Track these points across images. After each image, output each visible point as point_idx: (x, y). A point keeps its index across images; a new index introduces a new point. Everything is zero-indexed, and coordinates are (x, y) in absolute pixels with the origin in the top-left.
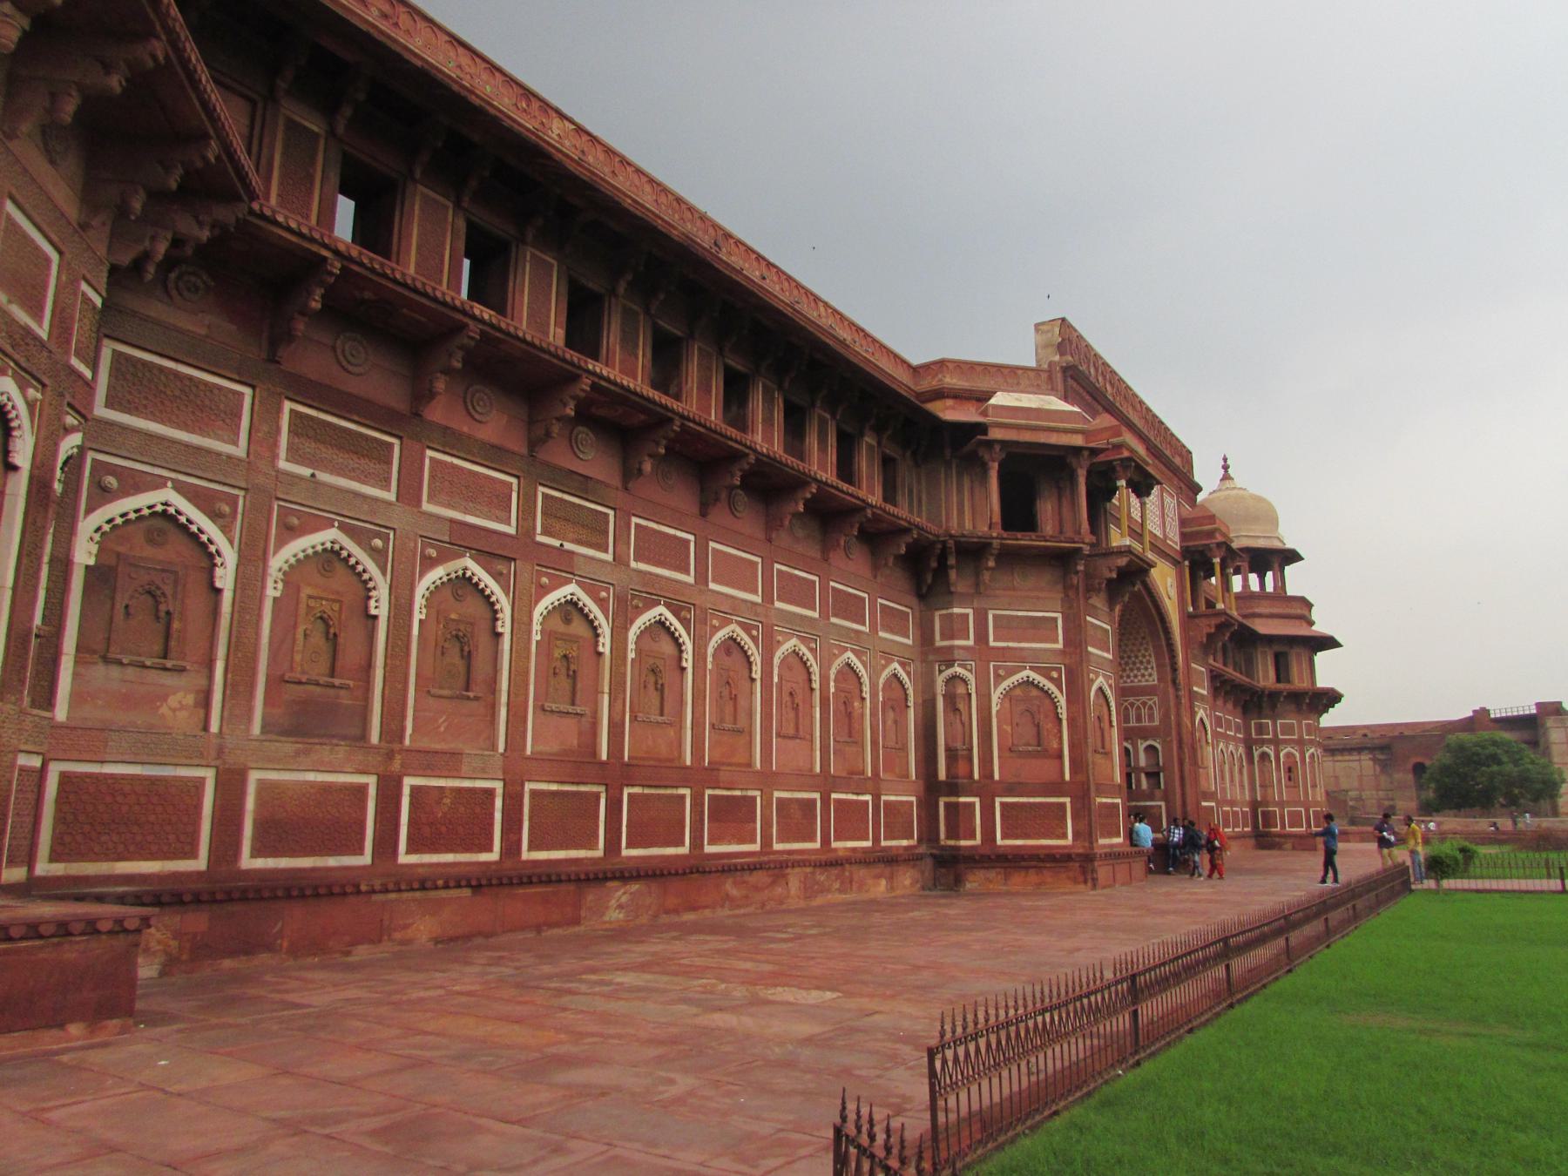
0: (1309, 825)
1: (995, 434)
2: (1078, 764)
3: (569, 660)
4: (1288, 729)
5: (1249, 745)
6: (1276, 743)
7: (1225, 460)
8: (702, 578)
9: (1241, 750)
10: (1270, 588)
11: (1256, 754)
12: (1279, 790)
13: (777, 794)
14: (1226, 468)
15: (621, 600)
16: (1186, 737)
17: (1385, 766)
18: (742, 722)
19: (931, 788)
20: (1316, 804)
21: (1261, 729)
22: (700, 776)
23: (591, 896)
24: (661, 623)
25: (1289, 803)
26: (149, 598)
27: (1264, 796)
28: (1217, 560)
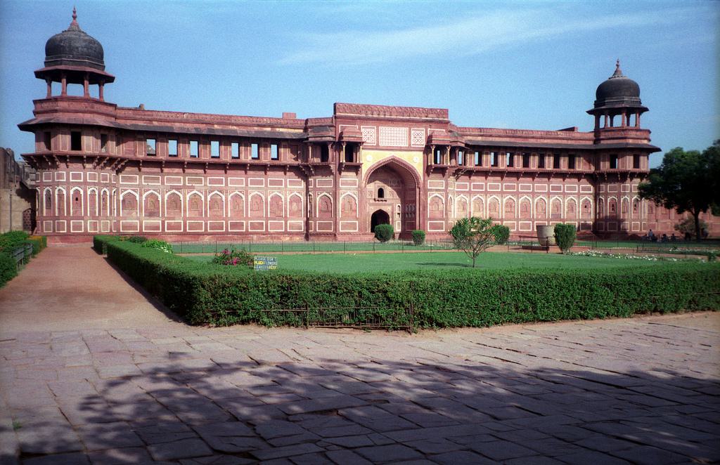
1: (310, 139)
3: (195, 202)
5: (596, 196)
8: (226, 184)
13: (244, 222)
14: (617, 65)
15: (206, 192)
18: (241, 208)
19: (308, 219)
22: (226, 219)
26: (129, 202)
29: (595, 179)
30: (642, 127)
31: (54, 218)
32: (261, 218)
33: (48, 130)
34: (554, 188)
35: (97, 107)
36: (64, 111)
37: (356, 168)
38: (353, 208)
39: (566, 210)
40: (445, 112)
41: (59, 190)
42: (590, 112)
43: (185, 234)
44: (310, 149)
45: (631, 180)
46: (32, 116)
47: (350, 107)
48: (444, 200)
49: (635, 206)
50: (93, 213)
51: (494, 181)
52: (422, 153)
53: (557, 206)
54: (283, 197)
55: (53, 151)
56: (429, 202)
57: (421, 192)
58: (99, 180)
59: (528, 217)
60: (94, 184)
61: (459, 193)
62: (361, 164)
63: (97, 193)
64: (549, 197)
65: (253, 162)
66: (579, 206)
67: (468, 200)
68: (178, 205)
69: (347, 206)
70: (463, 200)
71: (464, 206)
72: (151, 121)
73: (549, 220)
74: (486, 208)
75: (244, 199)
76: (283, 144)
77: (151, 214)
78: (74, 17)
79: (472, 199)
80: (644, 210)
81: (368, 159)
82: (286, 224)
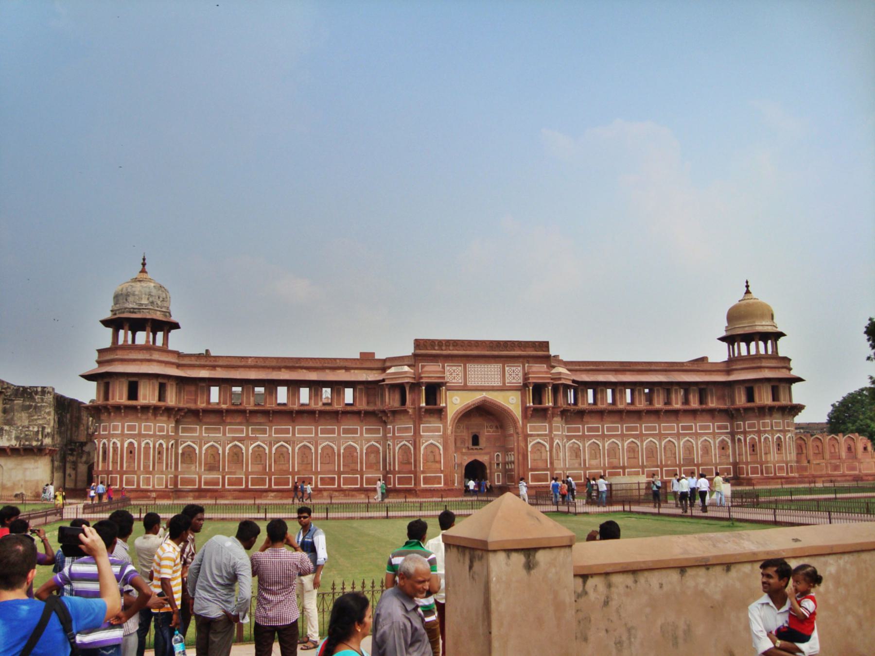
0: (762, 473)
1: (387, 382)
2: (415, 466)
5: (732, 434)
6: (745, 433)
7: (747, 282)
8: (294, 434)
10: (770, 352)
14: (747, 286)
15: (270, 443)
16: (521, 451)
18: (309, 461)
20: (767, 462)
21: (738, 427)
22: (293, 474)
23: (265, 494)
24: (282, 445)
25: (751, 463)
26: (189, 456)
29: (731, 414)
30: (781, 354)
31: (108, 473)
32: (334, 472)
33: (106, 380)
34: (684, 428)
35: (156, 356)
36: (123, 361)
37: (440, 413)
38: (437, 459)
40: (545, 345)
41: (114, 443)
42: (722, 339)
43: (247, 490)
44: (387, 390)
45: (771, 415)
46: (96, 365)
47: (432, 343)
48: (548, 446)
49: (779, 445)
50: (146, 467)
51: (613, 423)
52: (519, 393)
53: (689, 449)
54: (358, 448)
55: (111, 402)
56: (529, 449)
57: (520, 438)
58: (155, 432)
59: (655, 464)
60: (150, 436)
61: (569, 438)
62: (446, 407)
63: (151, 446)
64: (679, 439)
65: (323, 408)
66: (715, 449)
68: (240, 459)
69: (431, 458)
70: (576, 446)
71: (576, 453)
72: (214, 367)
73: (680, 466)
75: (313, 450)
76: (359, 387)
77: (212, 467)
78: (144, 264)
79: (587, 445)
80: (790, 450)
81: (455, 401)
82: (362, 478)
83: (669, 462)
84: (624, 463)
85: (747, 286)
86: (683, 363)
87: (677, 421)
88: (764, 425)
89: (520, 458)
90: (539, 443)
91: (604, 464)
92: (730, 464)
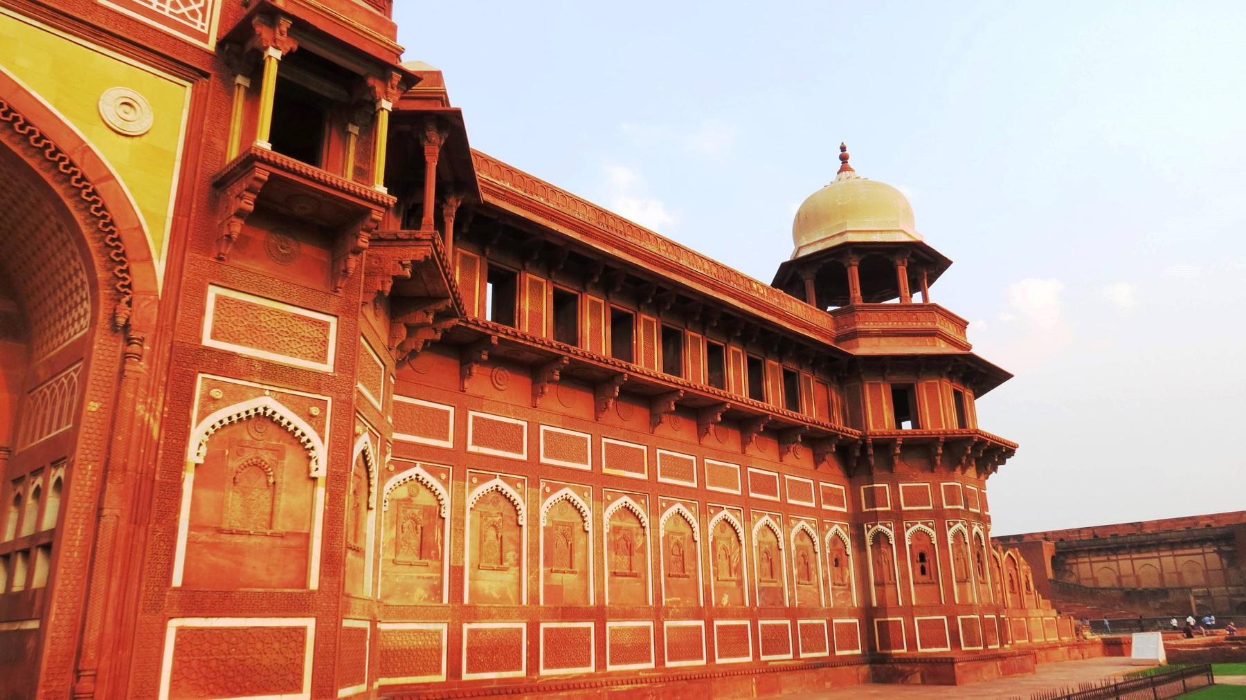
0: (956, 643)
4: (916, 496)
5: (857, 524)
6: (898, 517)
7: (843, 149)
9: (838, 528)
11: (868, 536)
12: (907, 588)
14: (844, 158)
17: (1232, 559)
20: (969, 608)
21: (872, 499)
25: (921, 609)
27: (881, 598)
28: (274, 54)
29: (857, 458)
39: (795, 572)
48: (321, 452)
49: (978, 556)
51: (570, 421)
52: (178, 96)
53: (770, 558)
56: (195, 453)
59: (690, 602)
61: (405, 455)
64: (748, 518)
67: (447, 502)
70: (424, 498)
74: (534, 552)
79: (470, 500)
83: (725, 600)
84: (600, 596)
85: (844, 158)
86: (750, 280)
87: (742, 457)
88: (952, 496)
89: (114, 508)
90: (264, 418)
91: (534, 599)
92: (852, 613)
